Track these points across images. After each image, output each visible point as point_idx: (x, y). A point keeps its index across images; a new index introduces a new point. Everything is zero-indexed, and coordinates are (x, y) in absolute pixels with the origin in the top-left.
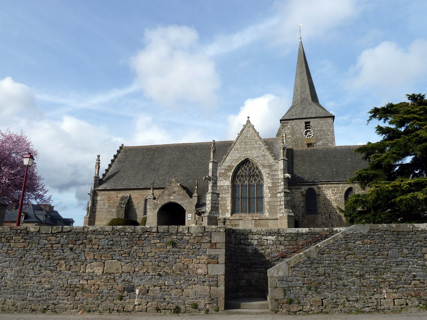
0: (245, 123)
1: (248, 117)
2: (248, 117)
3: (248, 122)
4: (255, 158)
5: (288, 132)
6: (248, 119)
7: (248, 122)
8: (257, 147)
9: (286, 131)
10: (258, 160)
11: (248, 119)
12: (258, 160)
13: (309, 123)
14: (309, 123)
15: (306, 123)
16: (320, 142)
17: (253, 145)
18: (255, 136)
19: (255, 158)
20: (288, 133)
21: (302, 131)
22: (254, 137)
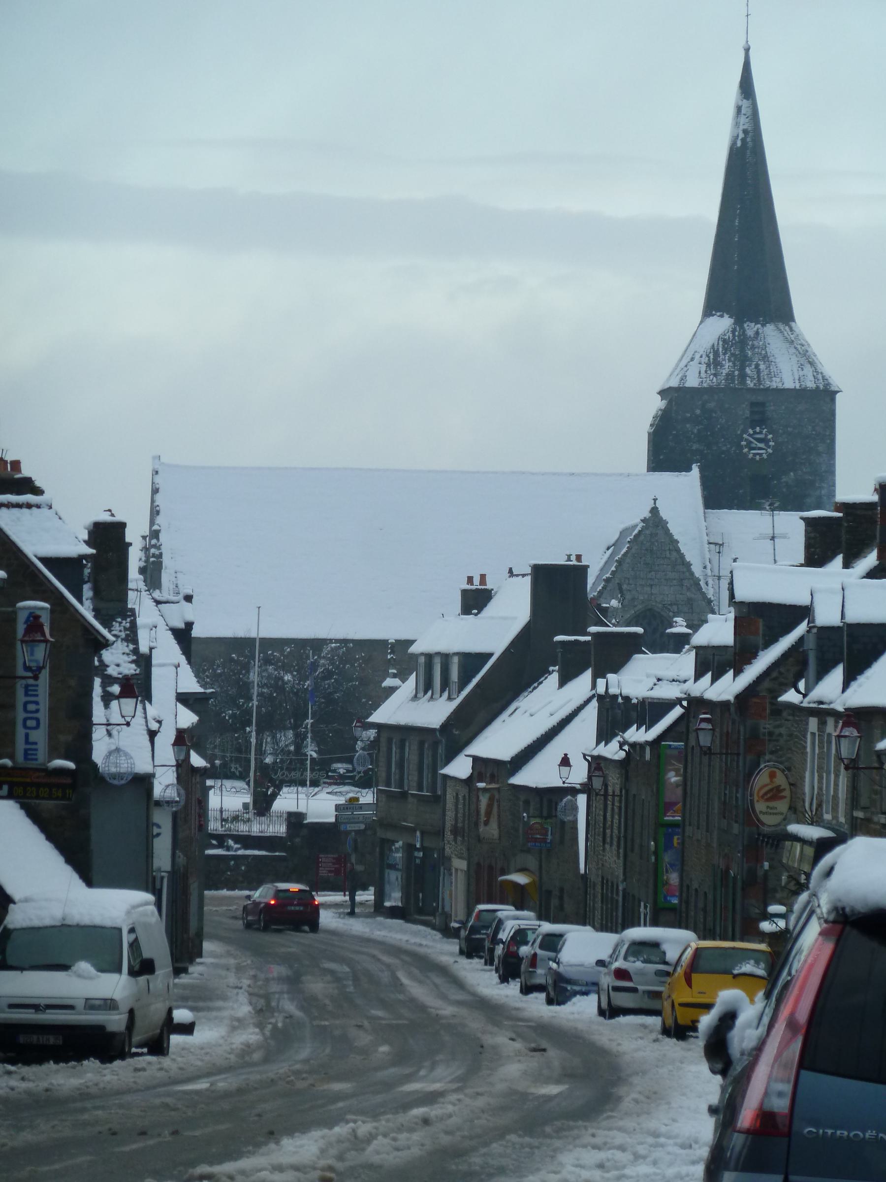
0: (647, 514)
1: (655, 500)
2: (655, 500)
3: (654, 511)
4: (669, 605)
5: (695, 431)
6: (655, 503)
7: (654, 511)
8: (675, 579)
9: (688, 426)
10: (676, 610)
11: (655, 503)
12: (676, 610)
13: (763, 404)
14: (763, 404)
15: (753, 404)
16: (792, 474)
17: (664, 573)
18: (669, 550)
19: (669, 605)
20: (693, 433)
21: (739, 432)
22: (668, 552)
